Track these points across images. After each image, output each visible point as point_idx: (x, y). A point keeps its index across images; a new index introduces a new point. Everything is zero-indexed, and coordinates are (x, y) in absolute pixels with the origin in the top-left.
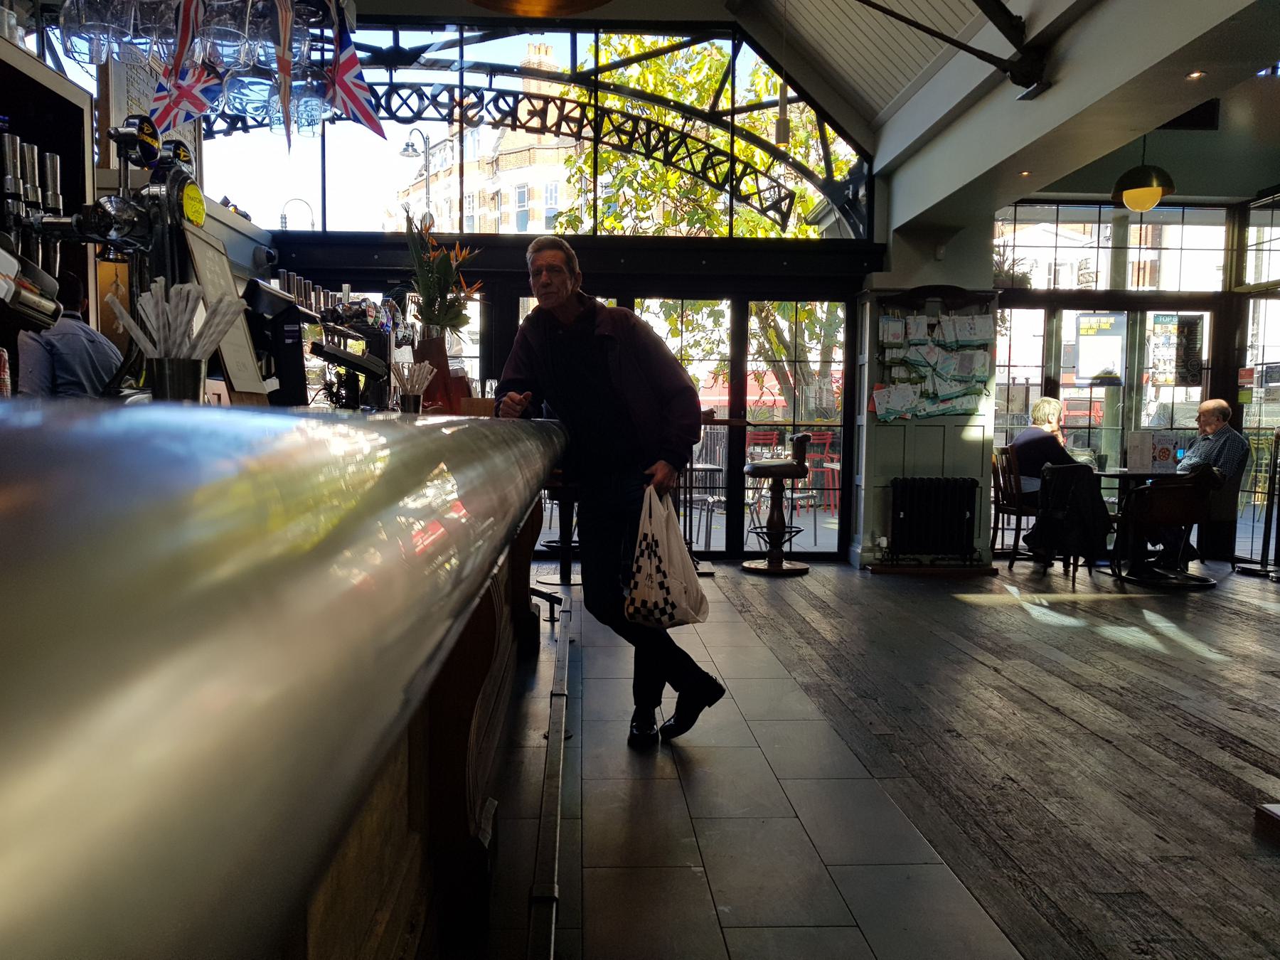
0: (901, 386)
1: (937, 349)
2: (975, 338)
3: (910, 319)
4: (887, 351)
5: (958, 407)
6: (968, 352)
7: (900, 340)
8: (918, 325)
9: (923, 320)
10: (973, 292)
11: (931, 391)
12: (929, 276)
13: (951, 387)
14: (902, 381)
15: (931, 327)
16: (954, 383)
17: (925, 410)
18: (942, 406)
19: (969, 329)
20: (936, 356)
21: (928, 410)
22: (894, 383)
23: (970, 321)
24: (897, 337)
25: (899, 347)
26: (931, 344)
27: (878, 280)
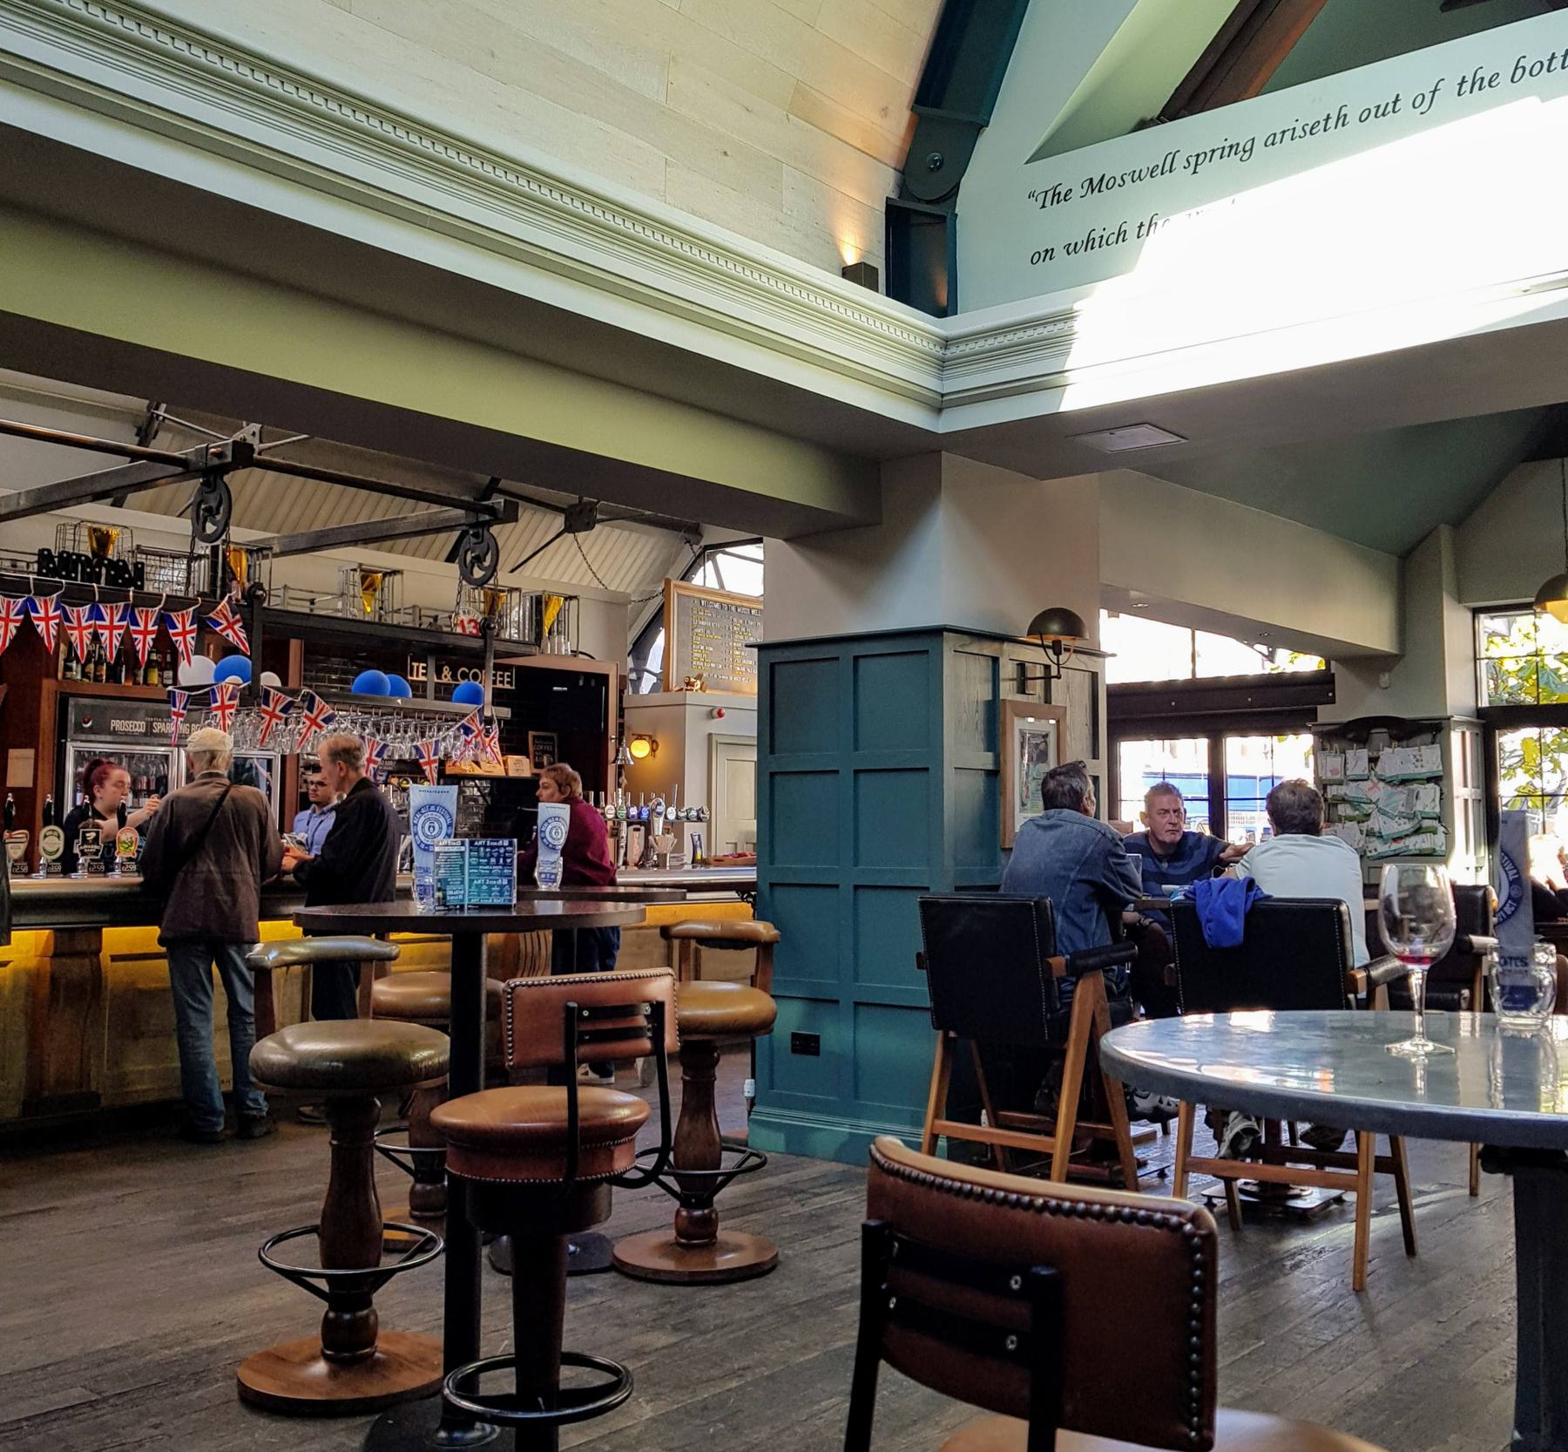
0: (1348, 824)
1: (1381, 784)
2: (1423, 770)
3: (1350, 753)
4: (1329, 788)
5: (1411, 847)
6: (1415, 786)
7: (1338, 777)
8: (1358, 759)
9: (1364, 754)
10: (1414, 721)
11: (1376, 830)
12: (1374, 705)
13: (1400, 825)
14: (1351, 819)
15: (1373, 761)
16: (1403, 821)
17: (1376, 850)
18: (1395, 846)
19: (1414, 761)
20: (1380, 792)
21: (1379, 851)
22: (1340, 821)
23: (1416, 753)
24: (1334, 772)
25: (1340, 783)
26: (1375, 780)
27: (1326, 714)
